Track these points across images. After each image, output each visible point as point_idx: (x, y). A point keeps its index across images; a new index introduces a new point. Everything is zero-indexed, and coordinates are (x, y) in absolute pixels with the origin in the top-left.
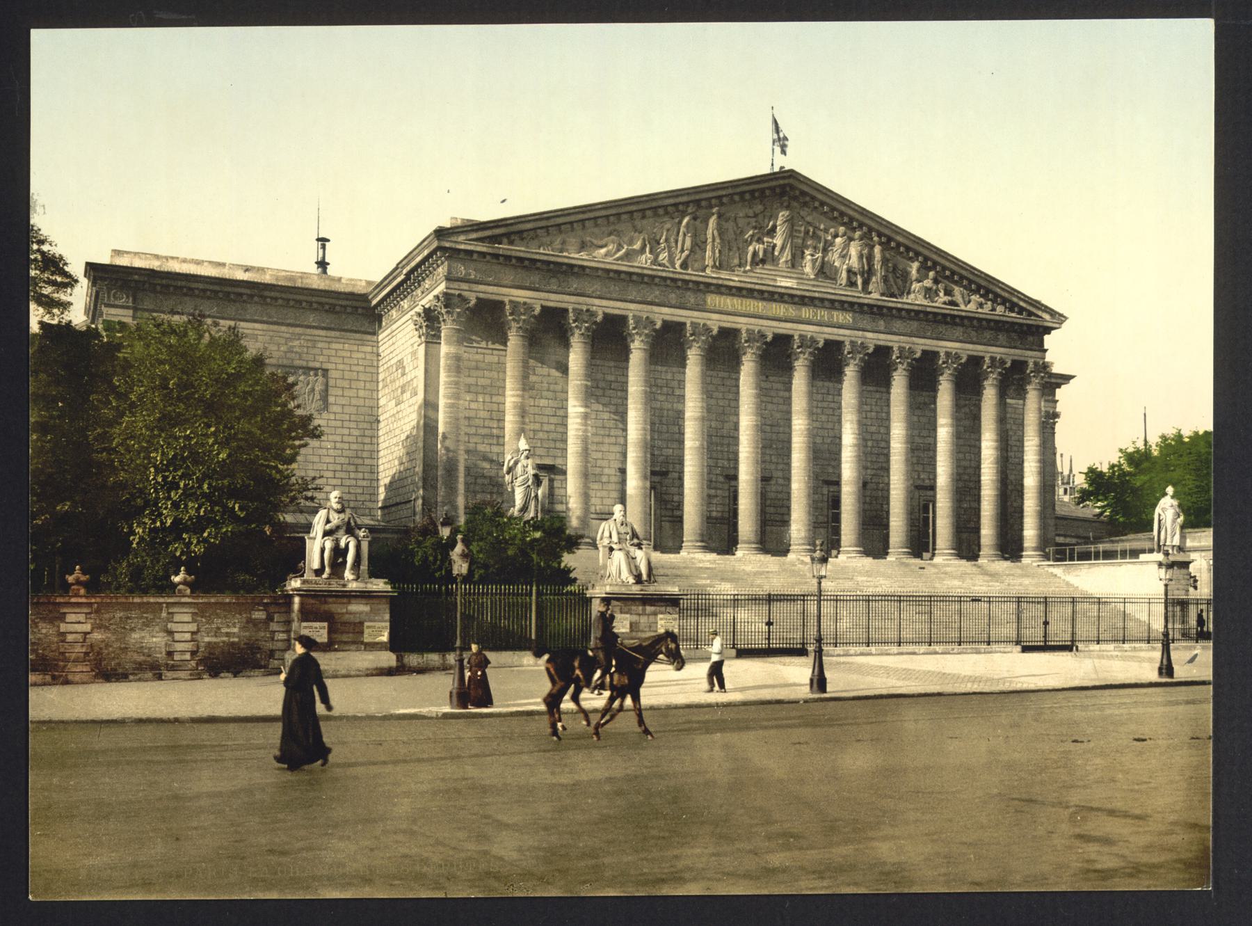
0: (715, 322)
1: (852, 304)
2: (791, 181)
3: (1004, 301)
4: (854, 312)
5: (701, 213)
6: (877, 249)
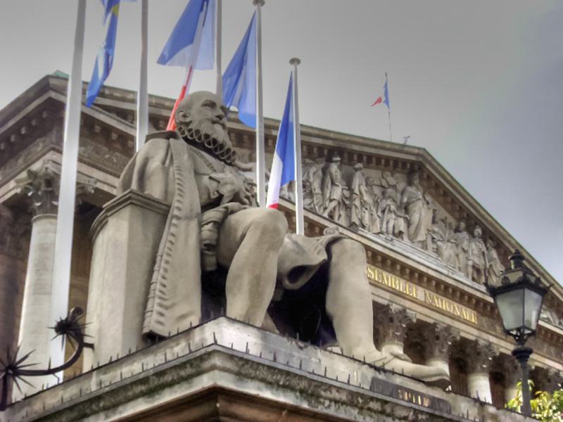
1: (479, 300)
2: (421, 159)
4: (478, 312)
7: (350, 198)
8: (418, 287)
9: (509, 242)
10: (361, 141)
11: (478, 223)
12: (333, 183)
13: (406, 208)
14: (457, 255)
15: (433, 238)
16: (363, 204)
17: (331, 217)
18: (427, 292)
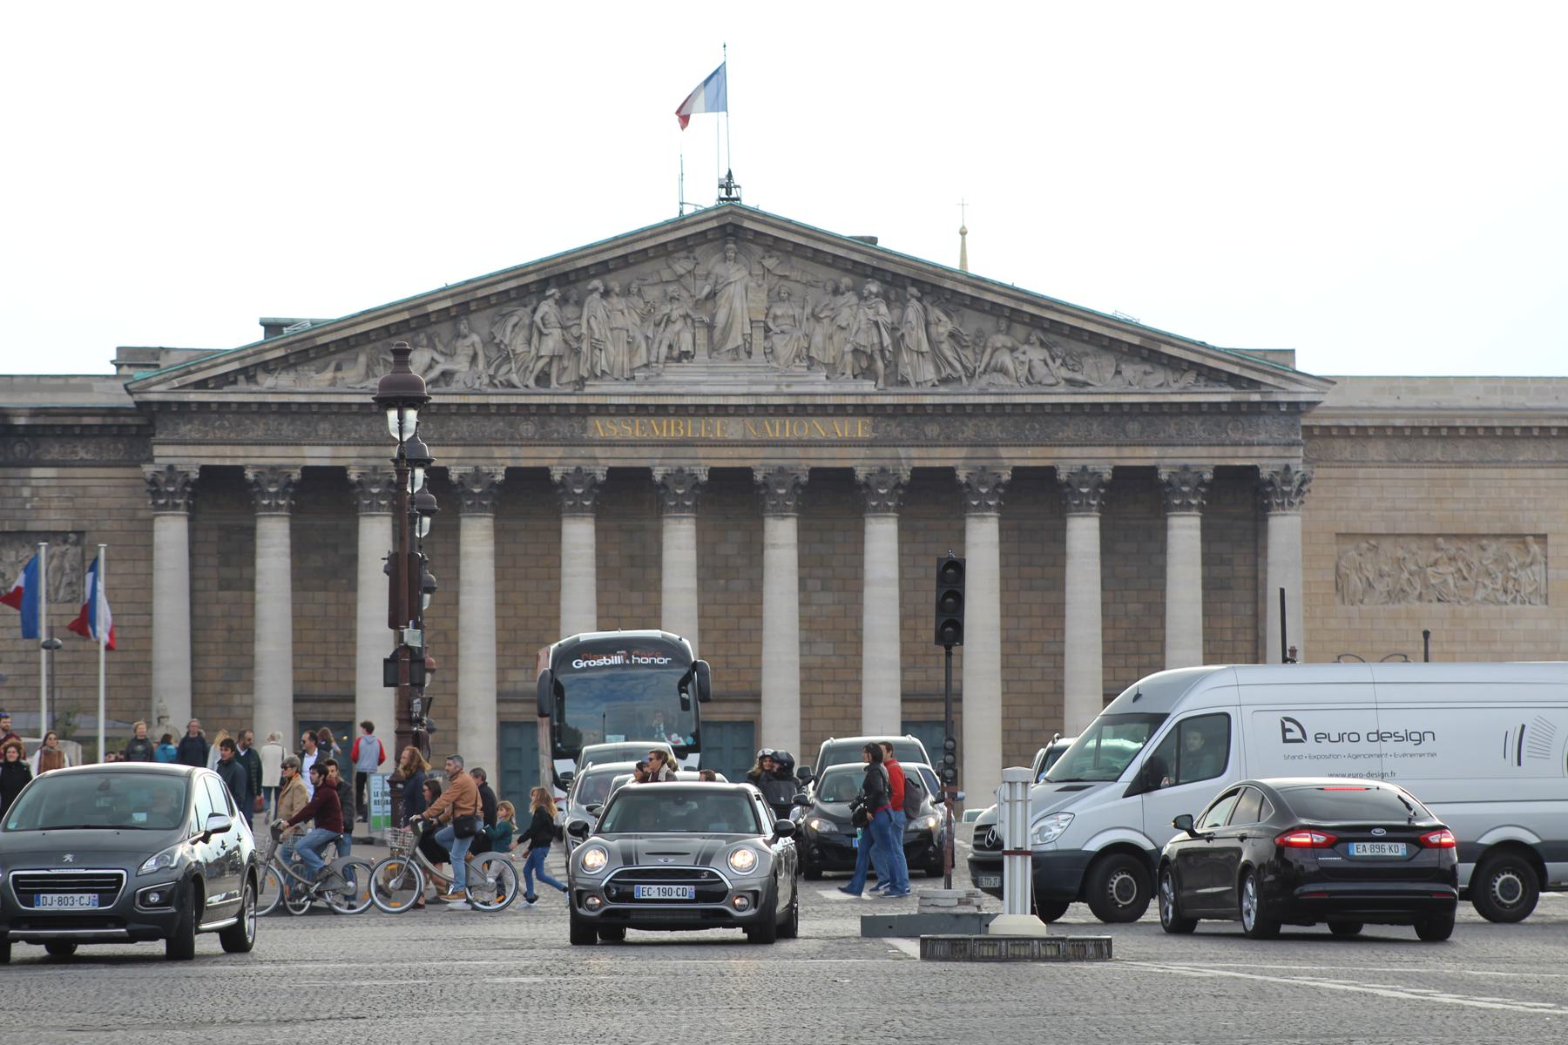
0: (601, 462)
2: (730, 219)
3: (1192, 364)
5: (573, 294)
6: (913, 311)
7: (578, 339)
8: (726, 420)
11: (876, 273)
12: (541, 334)
13: (712, 295)
14: (831, 338)
15: (767, 330)
16: (596, 346)
17: (543, 379)
18: (748, 420)
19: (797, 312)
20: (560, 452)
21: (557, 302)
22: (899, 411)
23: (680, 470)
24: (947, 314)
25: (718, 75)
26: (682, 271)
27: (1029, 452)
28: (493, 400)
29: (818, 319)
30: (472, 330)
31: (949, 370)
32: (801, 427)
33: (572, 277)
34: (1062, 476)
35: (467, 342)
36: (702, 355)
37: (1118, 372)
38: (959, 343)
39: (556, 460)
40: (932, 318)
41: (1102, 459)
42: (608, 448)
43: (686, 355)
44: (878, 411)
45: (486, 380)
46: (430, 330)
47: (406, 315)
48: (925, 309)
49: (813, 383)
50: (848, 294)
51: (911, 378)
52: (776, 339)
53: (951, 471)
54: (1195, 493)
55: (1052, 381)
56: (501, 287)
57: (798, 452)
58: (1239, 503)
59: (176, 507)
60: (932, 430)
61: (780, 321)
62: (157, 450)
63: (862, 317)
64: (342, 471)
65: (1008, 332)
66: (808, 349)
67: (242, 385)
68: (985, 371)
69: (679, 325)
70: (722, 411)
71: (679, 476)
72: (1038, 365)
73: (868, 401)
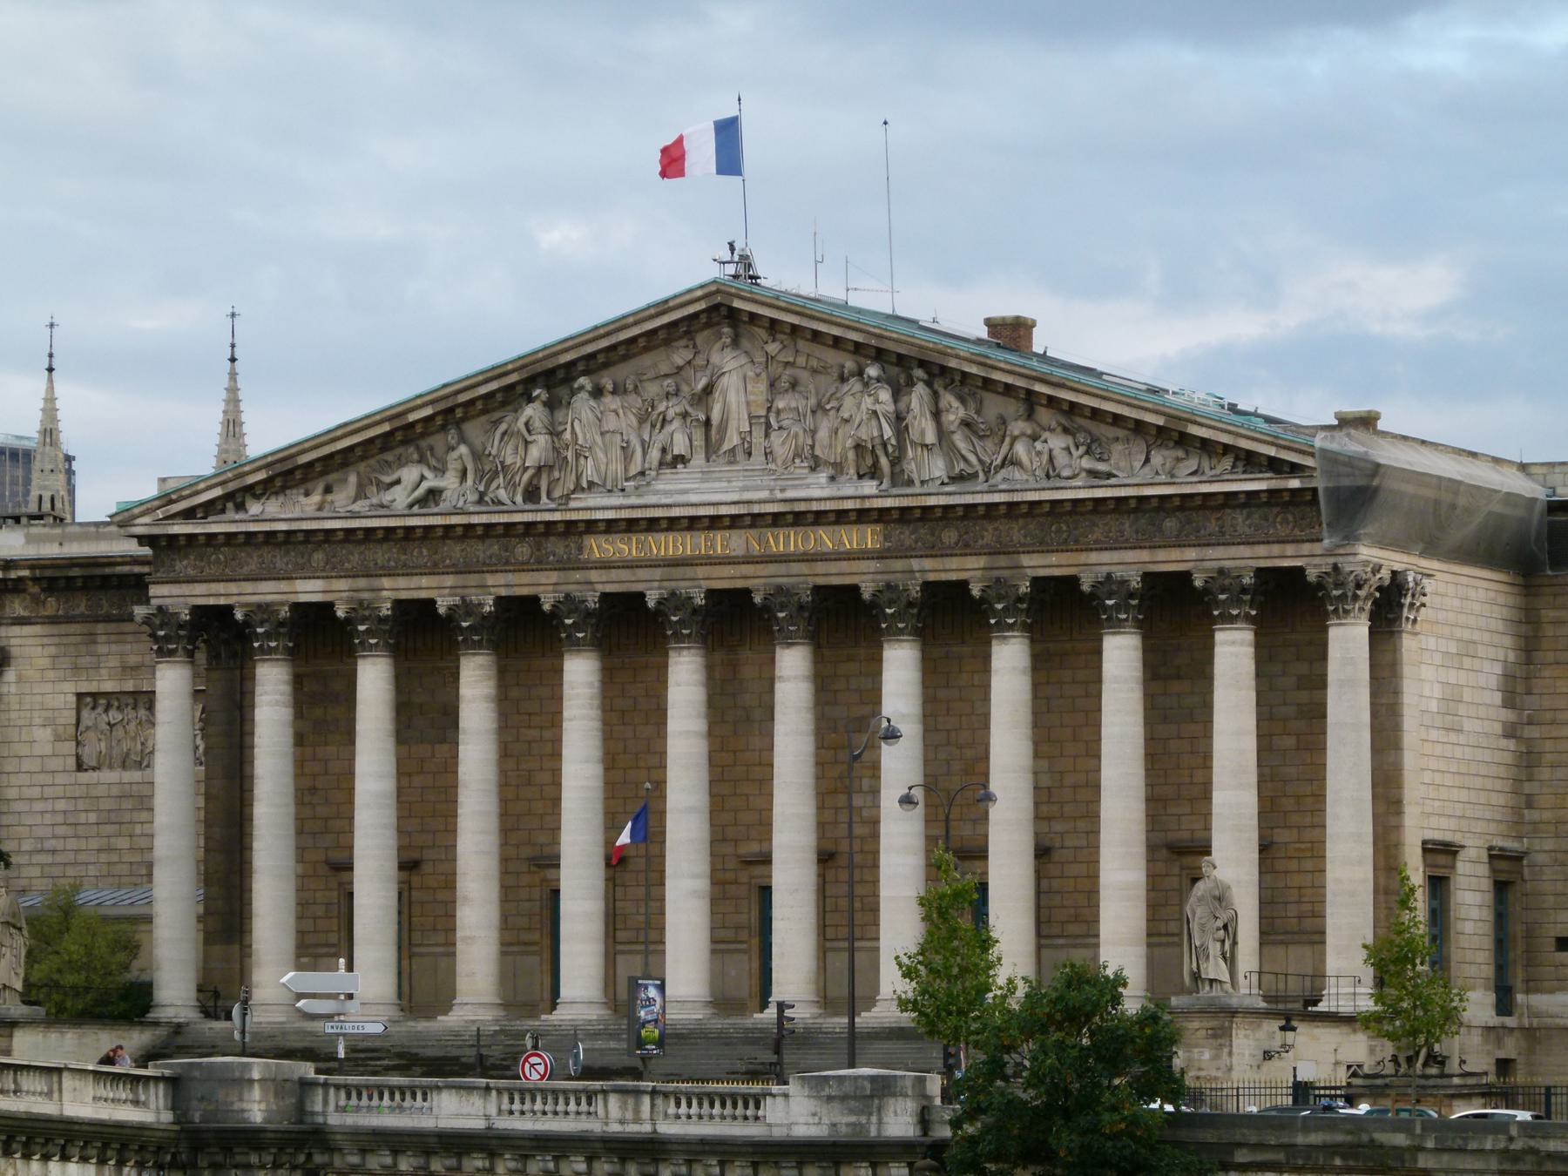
3: (1227, 449)
4: (887, 522)
6: (918, 397)
8: (727, 533)
9: (957, 357)
10: (570, 343)
11: (879, 355)
15: (768, 426)
17: (532, 494)
19: (801, 404)
20: (553, 577)
21: (545, 404)
22: (904, 515)
23: (673, 594)
24: (962, 401)
25: (728, 131)
26: (680, 362)
27: (1053, 559)
28: (475, 520)
29: (826, 412)
30: (463, 439)
31: (962, 465)
32: (805, 539)
33: (561, 374)
34: (1086, 588)
35: (454, 455)
36: (698, 460)
37: (1147, 460)
38: (975, 433)
39: (546, 587)
40: (943, 404)
41: (1128, 564)
42: (608, 569)
43: (681, 459)
44: (882, 516)
45: (475, 497)
46: (423, 443)
47: (386, 427)
48: (936, 396)
49: (808, 486)
50: (852, 380)
51: (915, 476)
52: (773, 435)
53: (963, 585)
54: (1239, 603)
55: (1065, 473)
56: (483, 390)
57: (803, 568)
58: (1290, 611)
59: (171, 653)
60: (950, 536)
61: (783, 416)
62: (154, 590)
63: (863, 407)
64: (328, 607)
65: (1030, 416)
66: (812, 447)
67: (231, 514)
68: (1003, 465)
69: (676, 424)
70: (714, 523)
71: (673, 600)
72: (1057, 452)
73: (867, 504)
